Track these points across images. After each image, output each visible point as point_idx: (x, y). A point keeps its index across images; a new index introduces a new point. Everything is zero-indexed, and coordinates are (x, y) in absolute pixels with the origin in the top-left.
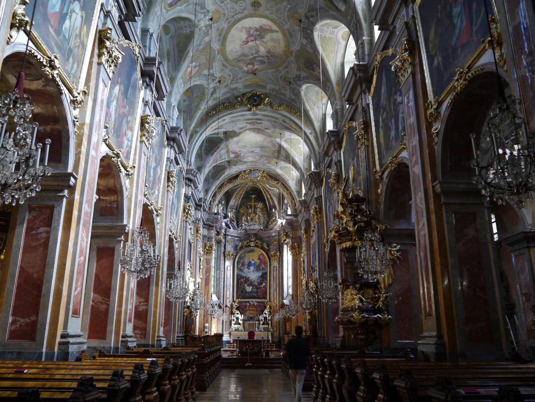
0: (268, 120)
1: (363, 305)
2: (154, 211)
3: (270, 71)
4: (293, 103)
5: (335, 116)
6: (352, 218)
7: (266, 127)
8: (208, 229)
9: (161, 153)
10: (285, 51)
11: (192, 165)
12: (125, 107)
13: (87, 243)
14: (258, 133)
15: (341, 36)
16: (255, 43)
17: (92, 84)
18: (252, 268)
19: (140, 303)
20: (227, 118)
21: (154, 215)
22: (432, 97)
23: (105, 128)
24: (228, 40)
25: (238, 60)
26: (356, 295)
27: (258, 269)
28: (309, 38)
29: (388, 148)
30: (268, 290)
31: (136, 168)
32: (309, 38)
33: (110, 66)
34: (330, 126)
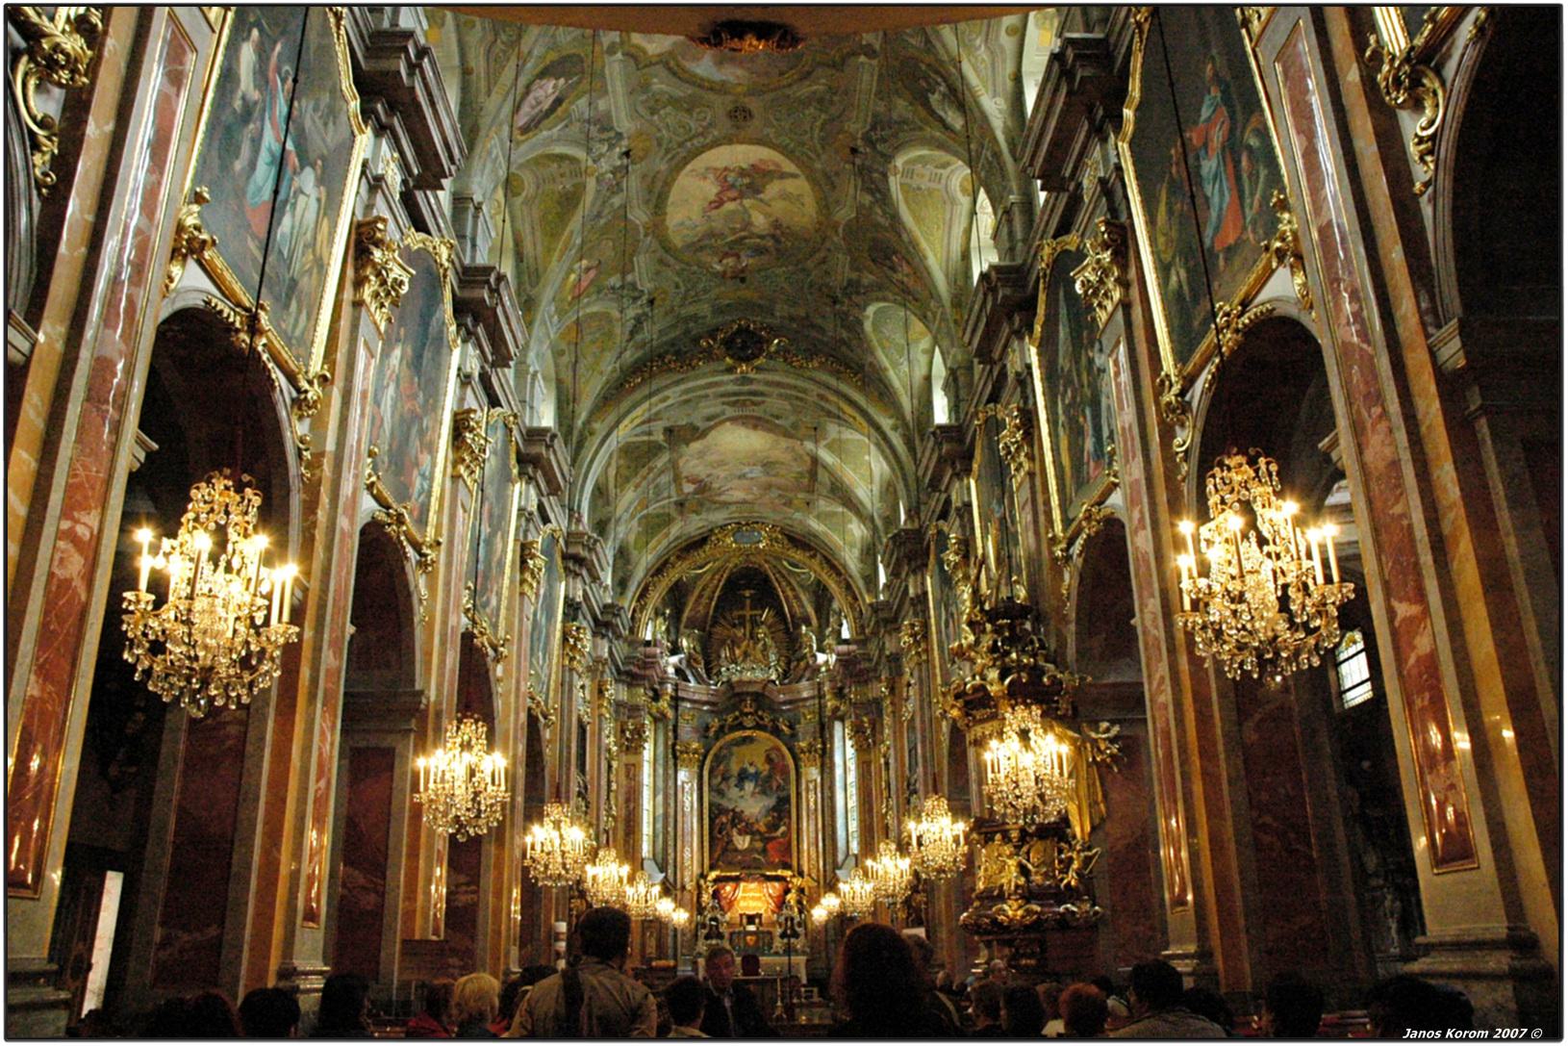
0: (780, 395)
1: (1028, 881)
2: (489, 650)
4: (844, 349)
5: (955, 384)
6: (995, 660)
7: (776, 412)
8: (630, 685)
9: (503, 499)
11: (585, 519)
12: (415, 397)
13: (332, 744)
14: (755, 427)
17: (341, 356)
18: (749, 786)
19: (457, 886)
20: (674, 394)
21: (489, 659)
22: (1171, 363)
23: (370, 456)
24: (671, 199)
25: (697, 247)
26: (1010, 857)
27: (764, 786)
28: (879, 191)
29: (1081, 481)
30: (794, 843)
31: (443, 547)
32: (879, 191)
33: (382, 305)
34: (941, 415)
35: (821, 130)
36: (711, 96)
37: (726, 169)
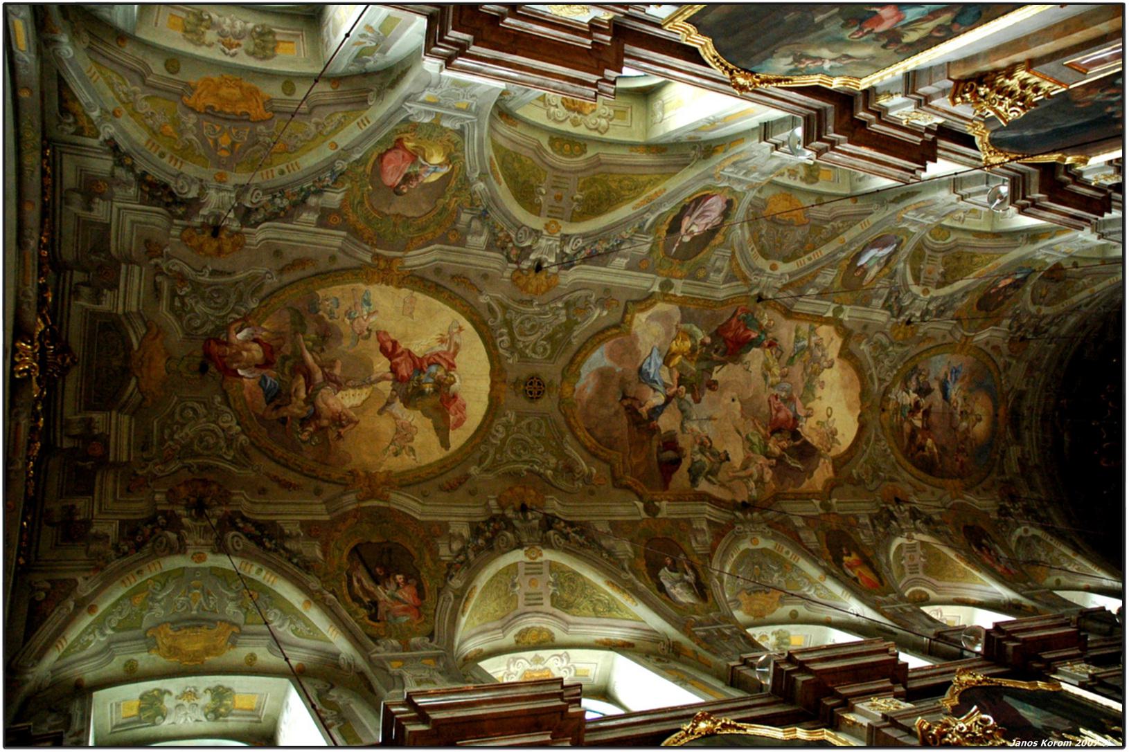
3: (229, 421)
10: (366, 472)
15: (529, 626)
16: (383, 378)
24: (420, 297)
28: (489, 541)
32: (489, 541)
35: (528, 470)
36: (562, 361)
37: (452, 366)
